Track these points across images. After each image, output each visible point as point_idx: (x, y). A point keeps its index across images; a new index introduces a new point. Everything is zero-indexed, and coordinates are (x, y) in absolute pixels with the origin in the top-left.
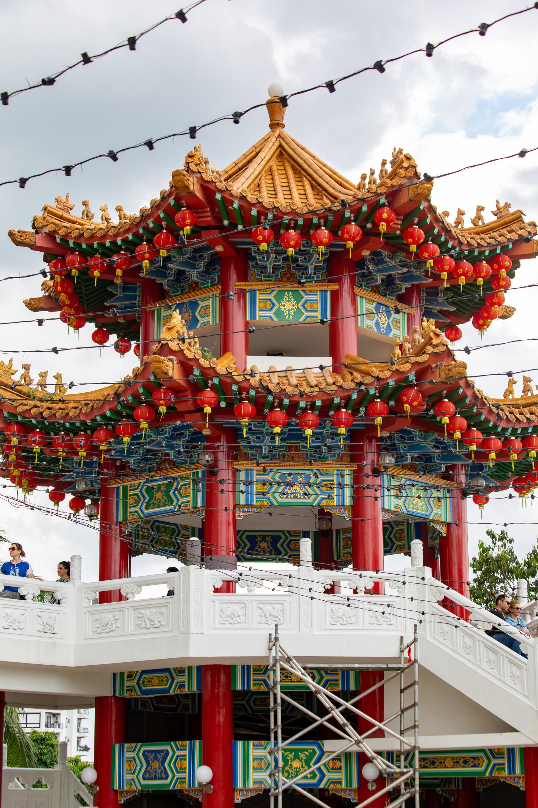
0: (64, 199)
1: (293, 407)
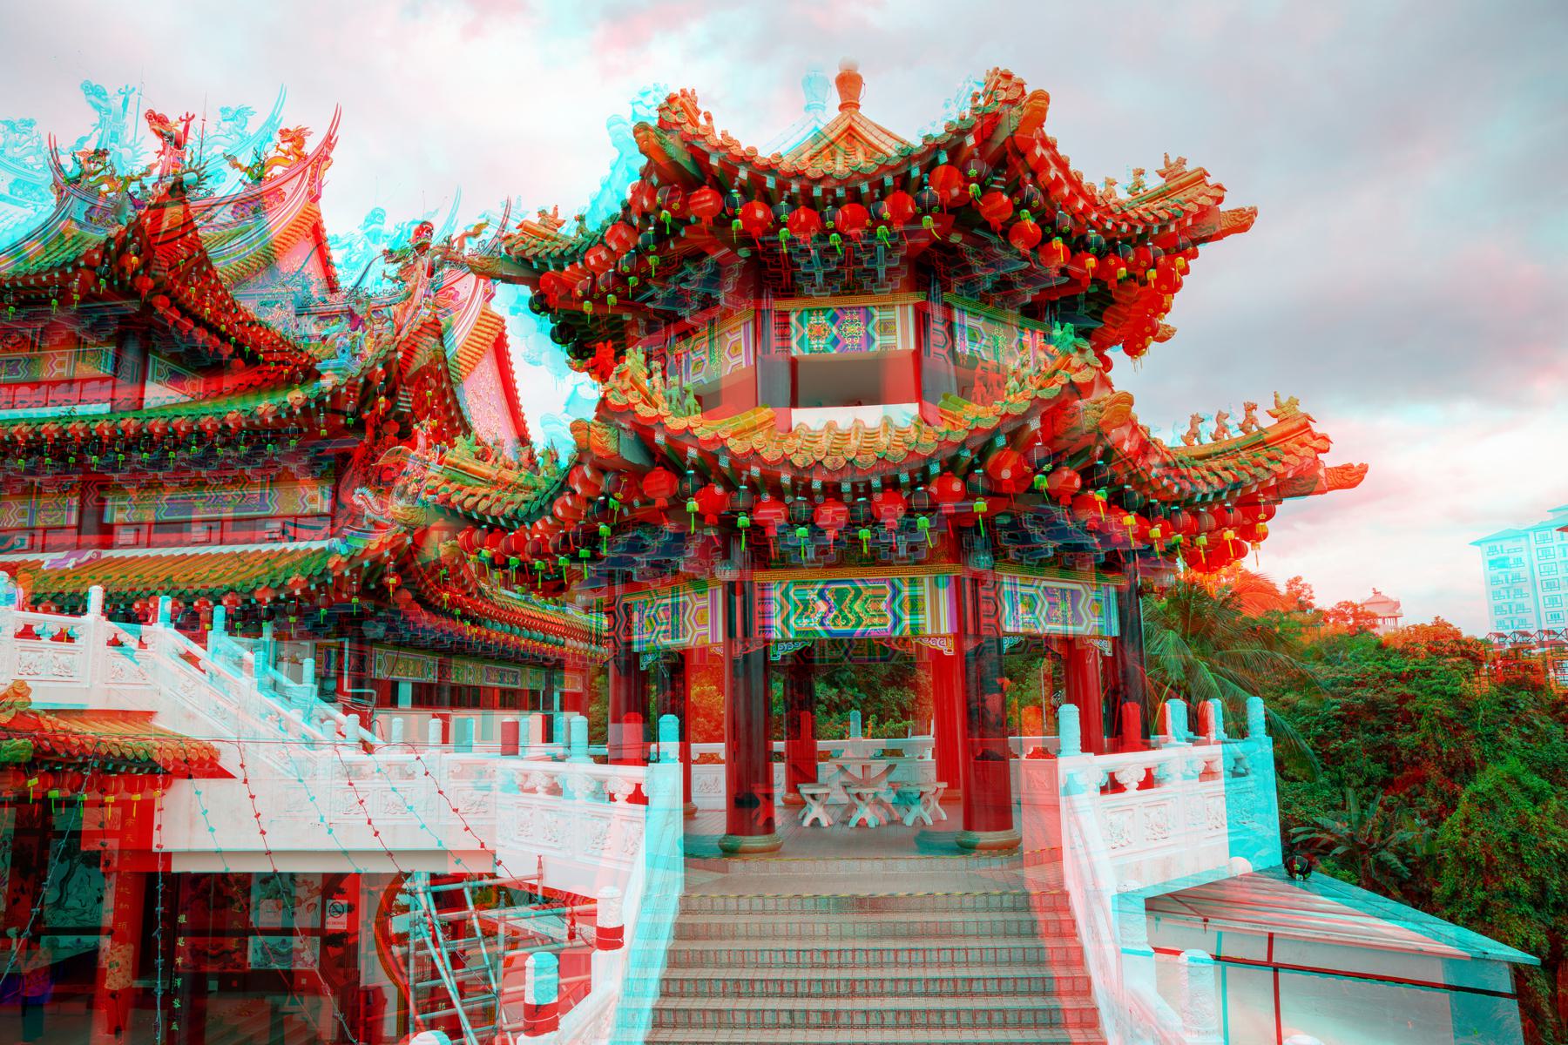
0: (550, 212)
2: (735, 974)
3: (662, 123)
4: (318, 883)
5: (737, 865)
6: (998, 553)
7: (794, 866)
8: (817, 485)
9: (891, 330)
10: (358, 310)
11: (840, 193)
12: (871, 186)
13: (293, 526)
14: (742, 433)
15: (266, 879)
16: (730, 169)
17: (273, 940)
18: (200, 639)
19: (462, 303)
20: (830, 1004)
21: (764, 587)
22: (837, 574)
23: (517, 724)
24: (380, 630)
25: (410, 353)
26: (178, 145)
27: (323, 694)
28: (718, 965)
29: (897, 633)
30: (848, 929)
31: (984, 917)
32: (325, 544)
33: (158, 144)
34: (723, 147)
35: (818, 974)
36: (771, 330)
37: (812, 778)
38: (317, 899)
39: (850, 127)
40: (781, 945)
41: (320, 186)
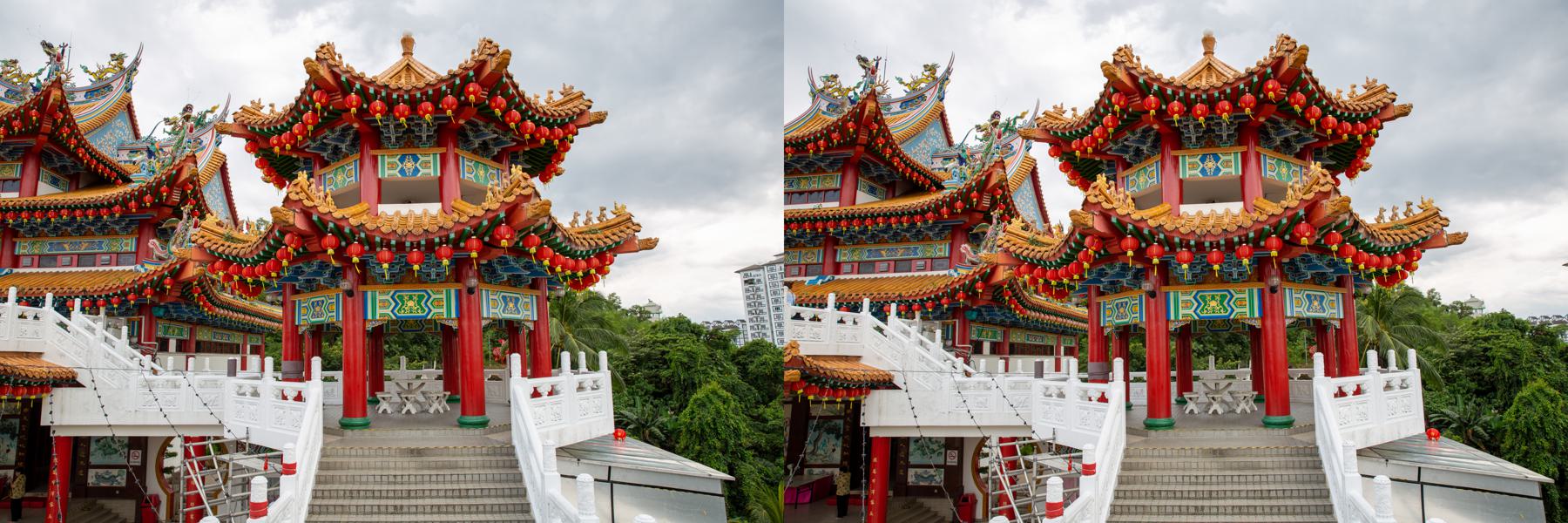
1: (400, 246)
5: (349, 433)
6: (480, 277)
14: (353, 215)
16: (351, 84)
21: (364, 294)
22: (400, 287)
36: (368, 163)
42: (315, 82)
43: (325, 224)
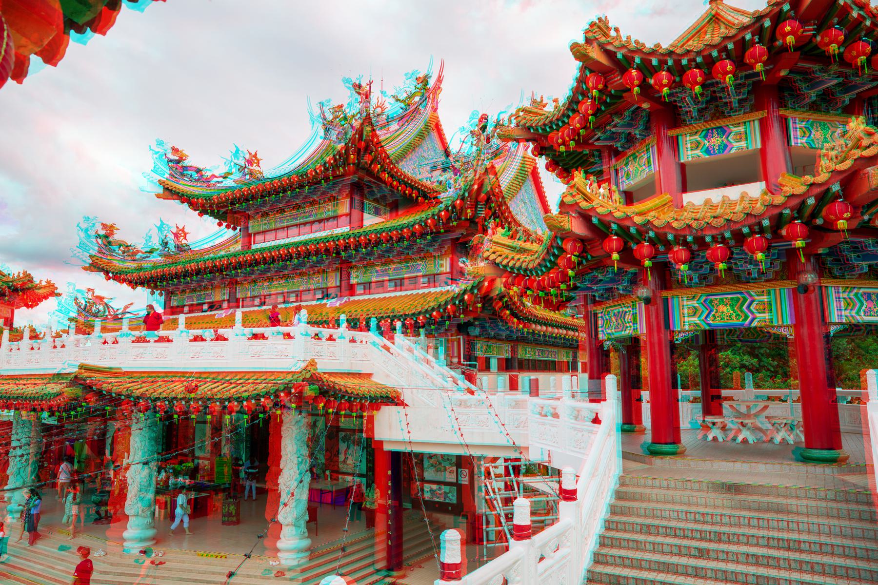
0: (539, 100)
1: (700, 241)
2: (648, 521)
3: (588, 41)
4: (454, 460)
5: (658, 461)
6: (822, 270)
7: (692, 463)
8: (690, 239)
9: (743, 138)
10: (457, 165)
11: (699, 60)
12: (719, 52)
13: (433, 279)
14: (652, 212)
15: (431, 456)
16: (629, 60)
17: (434, 487)
18: (391, 339)
19: (512, 154)
20: (705, 545)
23: (537, 380)
24: (477, 331)
25: (481, 186)
26: (367, 97)
27: (450, 365)
28: (638, 516)
29: (753, 325)
30: (719, 502)
31: (813, 503)
32: (448, 288)
33: (359, 98)
34: (624, 47)
35: (699, 527)
36: (666, 147)
37: (719, 413)
38: (454, 468)
39: (717, 14)
40: (677, 507)
41: (437, 103)
42: (589, 66)
43: (608, 226)
